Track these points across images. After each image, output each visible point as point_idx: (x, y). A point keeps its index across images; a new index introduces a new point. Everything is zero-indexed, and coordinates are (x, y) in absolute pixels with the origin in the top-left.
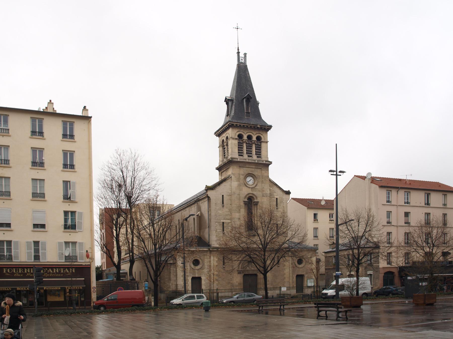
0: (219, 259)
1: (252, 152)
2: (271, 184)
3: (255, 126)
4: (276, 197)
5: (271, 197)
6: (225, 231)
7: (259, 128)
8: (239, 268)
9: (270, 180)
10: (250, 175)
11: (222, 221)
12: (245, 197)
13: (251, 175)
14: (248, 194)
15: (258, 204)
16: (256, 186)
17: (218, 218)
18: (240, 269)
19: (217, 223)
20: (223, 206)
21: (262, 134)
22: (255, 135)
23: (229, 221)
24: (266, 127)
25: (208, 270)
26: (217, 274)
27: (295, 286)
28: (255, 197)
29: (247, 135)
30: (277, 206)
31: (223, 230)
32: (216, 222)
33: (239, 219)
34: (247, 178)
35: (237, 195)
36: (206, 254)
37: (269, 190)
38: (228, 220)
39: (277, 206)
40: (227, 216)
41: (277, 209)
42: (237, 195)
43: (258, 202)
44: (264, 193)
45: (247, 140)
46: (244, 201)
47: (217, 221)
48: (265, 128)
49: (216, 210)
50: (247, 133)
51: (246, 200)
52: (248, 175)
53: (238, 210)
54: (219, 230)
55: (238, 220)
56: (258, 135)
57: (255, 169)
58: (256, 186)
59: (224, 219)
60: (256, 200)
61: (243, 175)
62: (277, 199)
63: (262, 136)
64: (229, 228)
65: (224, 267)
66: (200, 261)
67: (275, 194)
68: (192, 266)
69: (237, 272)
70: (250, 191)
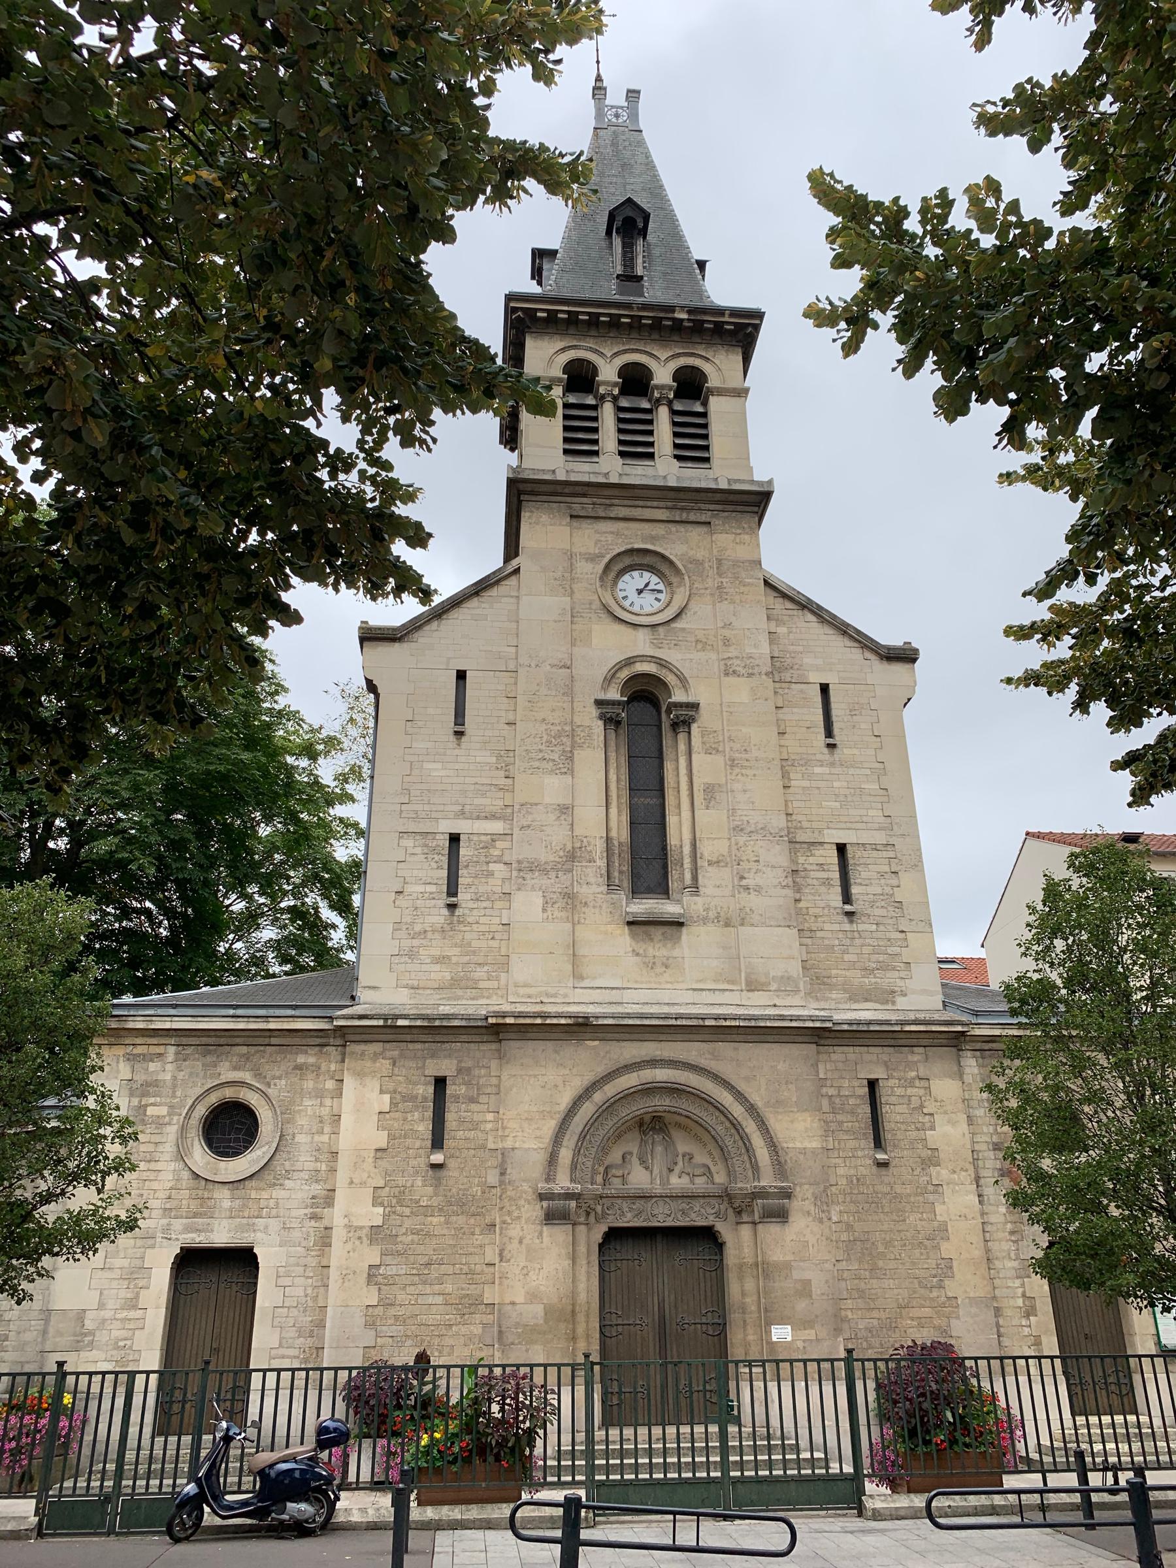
0: (406, 1098)
1: (656, 450)
2: (779, 605)
3: (662, 315)
4: (818, 678)
5: (787, 676)
6: (463, 896)
7: (686, 324)
8: (549, 1178)
9: (766, 583)
10: (637, 560)
11: (448, 826)
12: (609, 680)
13: (647, 560)
14: (629, 662)
15: (693, 719)
16: (678, 616)
17: (419, 807)
18: (563, 1182)
19: (408, 842)
20: (459, 734)
21: (707, 359)
22: (667, 360)
23: (497, 827)
24: (726, 319)
25: (317, 1189)
27: (1051, 1346)
28: (670, 679)
29: (620, 361)
30: (829, 733)
31: (452, 891)
33: (565, 810)
34: (626, 577)
35: (552, 666)
36: (311, 1060)
37: (764, 640)
38: (493, 817)
39: (829, 733)
40: (484, 795)
41: (832, 746)
42: (552, 666)
43: (695, 706)
44: (733, 652)
45: (615, 384)
46: (599, 703)
47: (412, 827)
48: (719, 326)
49: (407, 758)
50: (616, 354)
51: (614, 694)
52: (627, 561)
53: (556, 756)
54: (421, 888)
55: (552, 817)
56: (683, 361)
57: (673, 528)
58: (678, 616)
59: (462, 814)
60: (678, 696)
61: (592, 558)
62: (825, 689)
63: (706, 368)
64: (491, 874)
65: (436, 1167)
66: (264, 1115)
67: (808, 660)
68: (200, 1156)
69: (535, 1211)
70: (641, 643)
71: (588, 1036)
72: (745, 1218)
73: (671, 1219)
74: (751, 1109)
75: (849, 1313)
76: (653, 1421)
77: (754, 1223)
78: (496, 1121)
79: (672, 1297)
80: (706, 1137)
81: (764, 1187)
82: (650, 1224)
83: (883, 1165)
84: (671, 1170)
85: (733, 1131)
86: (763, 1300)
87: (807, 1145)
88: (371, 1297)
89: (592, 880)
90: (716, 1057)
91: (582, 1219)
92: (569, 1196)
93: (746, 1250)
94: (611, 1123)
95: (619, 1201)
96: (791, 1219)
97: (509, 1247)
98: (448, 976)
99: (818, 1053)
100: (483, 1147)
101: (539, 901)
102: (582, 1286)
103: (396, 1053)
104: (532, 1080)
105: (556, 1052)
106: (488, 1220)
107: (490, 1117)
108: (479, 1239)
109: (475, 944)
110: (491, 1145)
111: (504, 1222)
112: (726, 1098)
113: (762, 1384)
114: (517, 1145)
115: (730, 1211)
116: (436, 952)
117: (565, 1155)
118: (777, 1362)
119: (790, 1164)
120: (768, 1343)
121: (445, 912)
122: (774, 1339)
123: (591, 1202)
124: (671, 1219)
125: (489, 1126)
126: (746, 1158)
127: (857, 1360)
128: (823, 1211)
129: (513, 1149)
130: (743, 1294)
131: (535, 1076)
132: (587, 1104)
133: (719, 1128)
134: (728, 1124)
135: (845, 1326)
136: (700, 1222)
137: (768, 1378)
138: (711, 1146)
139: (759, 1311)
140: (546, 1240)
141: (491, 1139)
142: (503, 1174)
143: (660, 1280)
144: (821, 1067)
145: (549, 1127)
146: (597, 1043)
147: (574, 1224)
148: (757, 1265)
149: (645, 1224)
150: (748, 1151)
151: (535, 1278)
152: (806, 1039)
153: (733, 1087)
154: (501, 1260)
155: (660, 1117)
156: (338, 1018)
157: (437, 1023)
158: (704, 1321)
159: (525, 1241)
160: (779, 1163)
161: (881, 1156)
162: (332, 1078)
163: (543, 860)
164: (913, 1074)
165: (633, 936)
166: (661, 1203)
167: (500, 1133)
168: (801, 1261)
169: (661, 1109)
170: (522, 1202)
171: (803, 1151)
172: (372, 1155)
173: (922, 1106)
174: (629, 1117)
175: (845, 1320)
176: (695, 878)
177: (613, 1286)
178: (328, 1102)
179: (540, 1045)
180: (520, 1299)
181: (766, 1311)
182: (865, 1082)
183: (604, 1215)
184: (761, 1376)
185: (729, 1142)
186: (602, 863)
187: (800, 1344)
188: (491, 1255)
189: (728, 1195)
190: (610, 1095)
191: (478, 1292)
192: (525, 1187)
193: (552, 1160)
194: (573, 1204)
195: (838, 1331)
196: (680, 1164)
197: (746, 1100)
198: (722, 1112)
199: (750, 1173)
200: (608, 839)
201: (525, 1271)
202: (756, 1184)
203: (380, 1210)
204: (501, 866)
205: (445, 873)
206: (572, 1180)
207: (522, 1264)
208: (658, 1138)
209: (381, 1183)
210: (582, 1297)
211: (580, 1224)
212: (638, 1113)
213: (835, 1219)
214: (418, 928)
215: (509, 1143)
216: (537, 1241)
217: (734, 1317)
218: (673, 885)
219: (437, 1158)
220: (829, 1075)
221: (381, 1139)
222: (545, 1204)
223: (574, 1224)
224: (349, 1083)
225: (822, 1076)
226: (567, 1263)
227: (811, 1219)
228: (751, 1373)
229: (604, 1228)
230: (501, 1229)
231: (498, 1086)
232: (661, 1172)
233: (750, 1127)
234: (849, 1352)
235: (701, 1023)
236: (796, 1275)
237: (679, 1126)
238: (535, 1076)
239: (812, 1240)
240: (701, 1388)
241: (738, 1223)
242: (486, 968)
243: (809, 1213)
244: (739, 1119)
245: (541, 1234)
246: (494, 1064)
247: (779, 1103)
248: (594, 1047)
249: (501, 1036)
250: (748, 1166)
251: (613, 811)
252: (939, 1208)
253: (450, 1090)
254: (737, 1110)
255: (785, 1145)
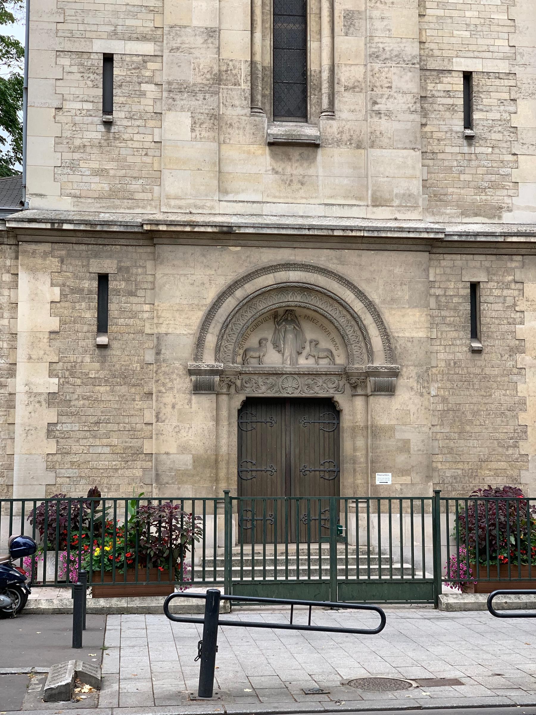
0: (73, 291)
6: (118, 114)
8: (197, 357)
17: (74, 27)
19: (65, 61)
23: (148, 48)
26: (55, 389)
31: (108, 109)
32: (60, 52)
38: (144, 38)
40: (135, 16)
47: (68, 46)
54: (78, 106)
55: (200, 40)
59: (114, 35)
64: (143, 94)
69: (187, 383)
71: (231, 242)
72: (359, 391)
73: (298, 391)
74: (370, 305)
75: (439, 466)
76: (279, 540)
77: (367, 396)
78: (152, 311)
79: (297, 451)
80: (330, 328)
81: (376, 368)
82: (281, 395)
83: (477, 352)
84: (299, 353)
85: (353, 323)
86: (370, 454)
87: (415, 334)
88: (51, 447)
89: (237, 103)
90: (342, 263)
91: (225, 390)
92: (213, 372)
93: (359, 417)
94: (249, 315)
95: (256, 377)
96: (397, 393)
97: (164, 411)
98: (106, 187)
99: (430, 259)
100: (142, 332)
101: (188, 122)
102: (224, 441)
103: (63, 253)
104: (182, 279)
105: (204, 255)
106: (146, 390)
107: (147, 307)
108: (139, 404)
109: (130, 159)
110: (147, 331)
111: (160, 392)
112: (349, 296)
113: (365, 515)
114: (170, 331)
115: (348, 386)
116: (95, 165)
117: (211, 340)
118: (379, 499)
119: (399, 350)
120: (372, 486)
121: (102, 128)
122: (378, 483)
123: (232, 377)
124: (298, 391)
125: (146, 315)
126: (363, 344)
127: (443, 499)
128: (424, 387)
129: (167, 334)
130: (355, 449)
131: (185, 275)
132: (230, 299)
133: (342, 320)
134: (349, 317)
135: (435, 474)
136: (322, 394)
137: (371, 510)
138: (334, 334)
139: (367, 463)
140: (194, 406)
141: (147, 325)
142: (158, 353)
143: (288, 438)
144: (432, 271)
145: (197, 317)
146: (239, 248)
147: (218, 394)
148: (367, 427)
149: (277, 395)
150: (365, 339)
151: (185, 435)
152: (421, 248)
153: (355, 287)
154: (157, 421)
155: (292, 311)
156: (10, 220)
157: (98, 228)
158: (322, 468)
159: (177, 407)
160: (390, 349)
161: (476, 345)
162: (8, 272)
163: (191, 81)
164: (510, 278)
165: (274, 156)
166: (290, 379)
167: (155, 321)
168: (403, 425)
169: (293, 304)
170: (174, 376)
171: (411, 340)
172: (47, 336)
173: (515, 305)
174: (265, 310)
175: (434, 470)
176: (332, 103)
177: (249, 442)
178: (6, 292)
179: (189, 249)
180: (173, 450)
181: (372, 462)
182: (468, 285)
183: (243, 387)
184: (366, 510)
185: (349, 332)
186: (246, 86)
187: (398, 487)
188: (149, 417)
189: (346, 373)
190: (249, 291)
191: (139, 444)
192: (177, 364)
193: (200, 343)
194: (217, 378)
195: (429, 477)
196: (308, 348)
197: (366, 298)
198: (345, 308)
199: (365, 357)
200: (253, 63)
201: (177, 430)
202: (370, 365)
203: (56, 380)
204: (152, 87)
205: (100, 92)
206: (216, 360)
207: (175, 424)
208: (290, 327)
209: (56, 359)
210: (224, 450)
211: (222, 394)
212: (274, 307)
213: (433, 393)
214: (77, 142)
215: (163, 330)
216: (187, 407)
217: (346, 466)
218: (312, 109)
219: (103, 340)
220: (438, 278)
221: (54, 324)
222: (193, 378)
223: (218, 394)
224: (23, 278)
225: (431, 279)
226: (211, 424)
227: (413, 393)
228: (357, 507)
229: (242, 398)
230: (157, 396)
231: (153, 283)
232: (291, 355)
233: (368, 320)
234: (437, 492)
235: (330, 233)
236: (398, 435)
237: (307, 317)
238: (185, 275)
239: (413, 408)
240: (317, 517)
241: (353, 396)
242: (141, 181)
243: (412, 388)
244: (359, 313)
245: (190, 401)
246: (149, 265)
247: (393, 300)
248: (237, 253)
249: (155, 241)
250: (364, 351)
251: (258, 35)
252: (521, 387)
253: (112, 285)
254: (358, 306)
255: (396, 335)
